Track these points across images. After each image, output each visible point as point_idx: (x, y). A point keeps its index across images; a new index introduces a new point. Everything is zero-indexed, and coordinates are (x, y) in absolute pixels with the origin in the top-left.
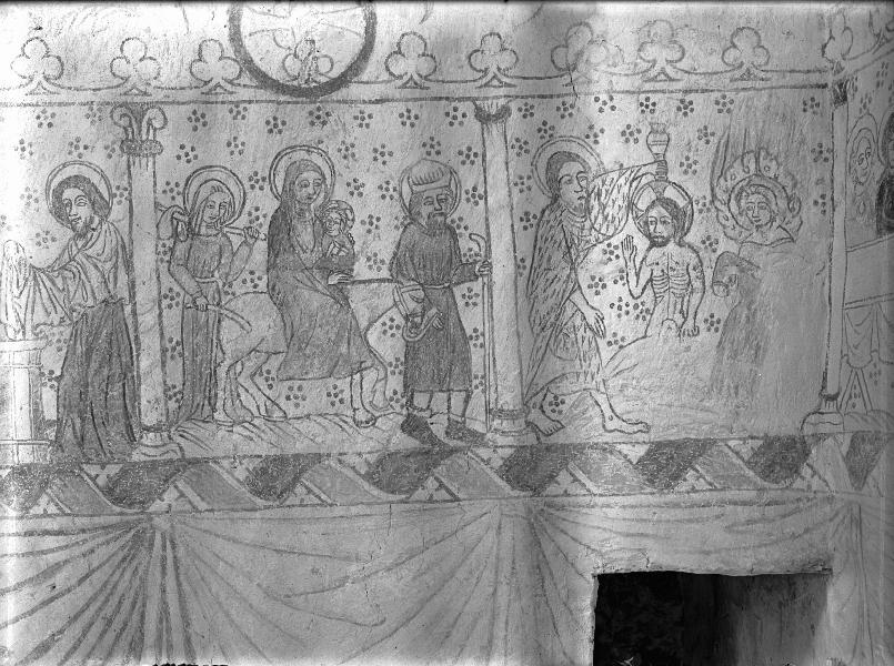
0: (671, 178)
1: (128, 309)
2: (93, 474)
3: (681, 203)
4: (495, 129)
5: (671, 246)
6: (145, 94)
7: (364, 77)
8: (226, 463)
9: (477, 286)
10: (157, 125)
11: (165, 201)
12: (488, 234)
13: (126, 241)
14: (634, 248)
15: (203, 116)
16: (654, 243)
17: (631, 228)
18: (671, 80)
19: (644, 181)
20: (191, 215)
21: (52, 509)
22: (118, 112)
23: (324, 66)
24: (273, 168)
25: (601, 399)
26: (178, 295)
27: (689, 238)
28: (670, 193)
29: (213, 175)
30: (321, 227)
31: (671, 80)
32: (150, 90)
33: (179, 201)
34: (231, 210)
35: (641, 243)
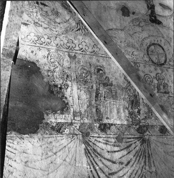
2: (135, 127)
7: (166, 64)
8: (155, 126)
10: (139, 66)
21: (128, 134)
23: (161, 61)
29: (148, 76)
30: (164, 87)
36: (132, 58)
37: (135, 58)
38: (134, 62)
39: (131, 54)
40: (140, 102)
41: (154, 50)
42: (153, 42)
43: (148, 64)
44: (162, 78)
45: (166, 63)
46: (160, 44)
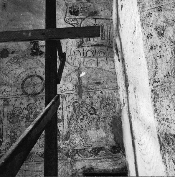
0: (93, 104)
1: (2, 130)
3: (96, 108)
4: (64, 99)
5: (94, 115)
6: (7, 97)
7: (43, 92)
9: (61, 123)
10: (9, 101)
11: (9, 113)
12: (63, 115)
13: (2, 119)
14: (87, 115)
15: (16, 100)
16: (91, 114)
17: (87, 112)
18: (93, 89)
19: (89, 105)
20: (13, 114)
22: (3, 100)
23: (36, 91)
24: (27, 106)
25: (83, 141)
26: (10, 127)
27: (97, 113)
28: (93, 106)
31: (93, 89)
32: (8, 96)
33: (12, 113)
34: (20, 113)
35: (89, 115)
36: (3, 95)
37: (6, 95)
38: (4, 99)
39: (2, 92)
40: (4, 134)
41: (31, 82)
42: (31, 74)
43: (21, 97)
44: (34, 107)
45: (42, 91)
46: (39, 74)
